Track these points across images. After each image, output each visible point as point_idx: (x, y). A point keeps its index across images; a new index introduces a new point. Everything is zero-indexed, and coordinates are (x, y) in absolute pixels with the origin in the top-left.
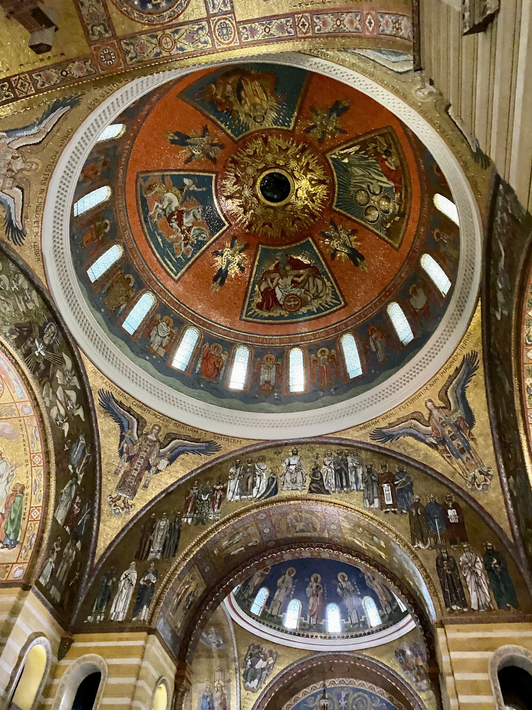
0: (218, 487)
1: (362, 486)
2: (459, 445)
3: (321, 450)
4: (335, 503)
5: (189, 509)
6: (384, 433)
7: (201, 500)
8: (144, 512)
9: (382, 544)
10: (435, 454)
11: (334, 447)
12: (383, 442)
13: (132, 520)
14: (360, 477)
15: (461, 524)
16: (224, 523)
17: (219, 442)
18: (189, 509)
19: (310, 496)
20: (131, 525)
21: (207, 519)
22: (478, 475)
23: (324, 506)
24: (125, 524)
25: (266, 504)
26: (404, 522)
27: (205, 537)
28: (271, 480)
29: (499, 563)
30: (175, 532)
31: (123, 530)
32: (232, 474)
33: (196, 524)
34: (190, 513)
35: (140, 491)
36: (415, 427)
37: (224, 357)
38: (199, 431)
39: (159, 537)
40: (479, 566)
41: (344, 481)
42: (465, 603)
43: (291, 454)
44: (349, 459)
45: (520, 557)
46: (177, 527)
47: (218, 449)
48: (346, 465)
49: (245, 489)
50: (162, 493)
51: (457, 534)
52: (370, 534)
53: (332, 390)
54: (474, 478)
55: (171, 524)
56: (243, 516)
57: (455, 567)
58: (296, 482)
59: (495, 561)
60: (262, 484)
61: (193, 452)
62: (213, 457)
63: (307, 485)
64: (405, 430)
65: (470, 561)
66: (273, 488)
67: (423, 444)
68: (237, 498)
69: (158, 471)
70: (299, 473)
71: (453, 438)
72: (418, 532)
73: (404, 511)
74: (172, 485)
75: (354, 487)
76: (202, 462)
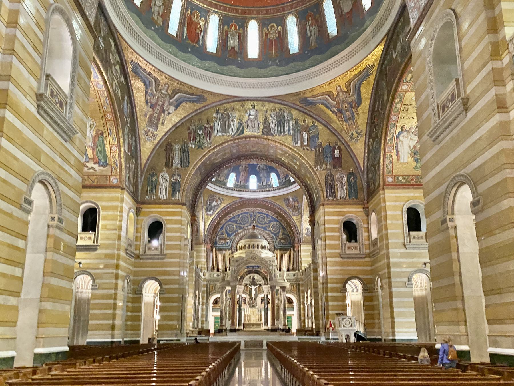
0: (207, 126)
1: (292, 132)
2: (348, 116)
3: (268, 106)
4: (276, 142)
5: (192, 139)
6: (308, 100)
7: (198, 134)
8: (164, 139)
9: (298, 163)
10: (335, 118)
11: (277, 106)
12: (306, 105)
13: (158, 143)
14: (291, 126)
15: (339, 159)
16: (214, 149)
17: (206, 96)
18: (192, 139)
19: (263, 136)
20: (158, 147)
21: (204, 146)
22: (354, 133)
23: (270, 142)
24: (154, 146)
25: (237, 139)
26: (312, 155)
27: (204, 156)
28: (240, 124)
29: (354, 178)
30: (185, 153)
31: (154, 149)
32: (215, 117)
33: (198, 149)
34: (193, 141)
35: (160, 126)
36: (327, 99)
37: (202, 23)
38: (193, 88)
39: (177, 155)
40: (345, 180)
41: (282, 128)
42: (335, 197)
43: (251, 107)
44: (286, 114)
45: (364, 177)
46: (186, 150)
47: (205, 100)
48: (284, 118)
49: (224, 129)
50: (173, 127)
51: (337, 163)
52: (292, 157)
53: (277, 61)
54: (352, 134)
55: (182, 148)
56: (224, 145)
57: (333, 180)
58: (254, 127)
59: (352, 178)
60: (234, 126)
61: (190, 101)
62: (202, 105)
63: (261, 128)
64: (321, 101)
65: (341, 177)
66: (241, 129)
68: (220, 134)
69: (169, 114)
70: (256, 121)
71: (347, 111)
72: (318, 162)
73: (313, 149)
74: (178, 122)
75: (287, 133)
76: (196, 108)
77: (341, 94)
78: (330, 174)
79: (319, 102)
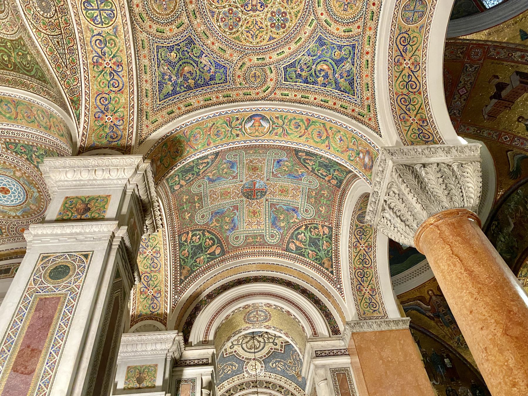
10: (433, 323)
15: (453, 368)
36: (419, 305)
64: (411, 307)
67: (424, 316)
77: (434, 298)
78: (450, 388)
79: (411, 309)
